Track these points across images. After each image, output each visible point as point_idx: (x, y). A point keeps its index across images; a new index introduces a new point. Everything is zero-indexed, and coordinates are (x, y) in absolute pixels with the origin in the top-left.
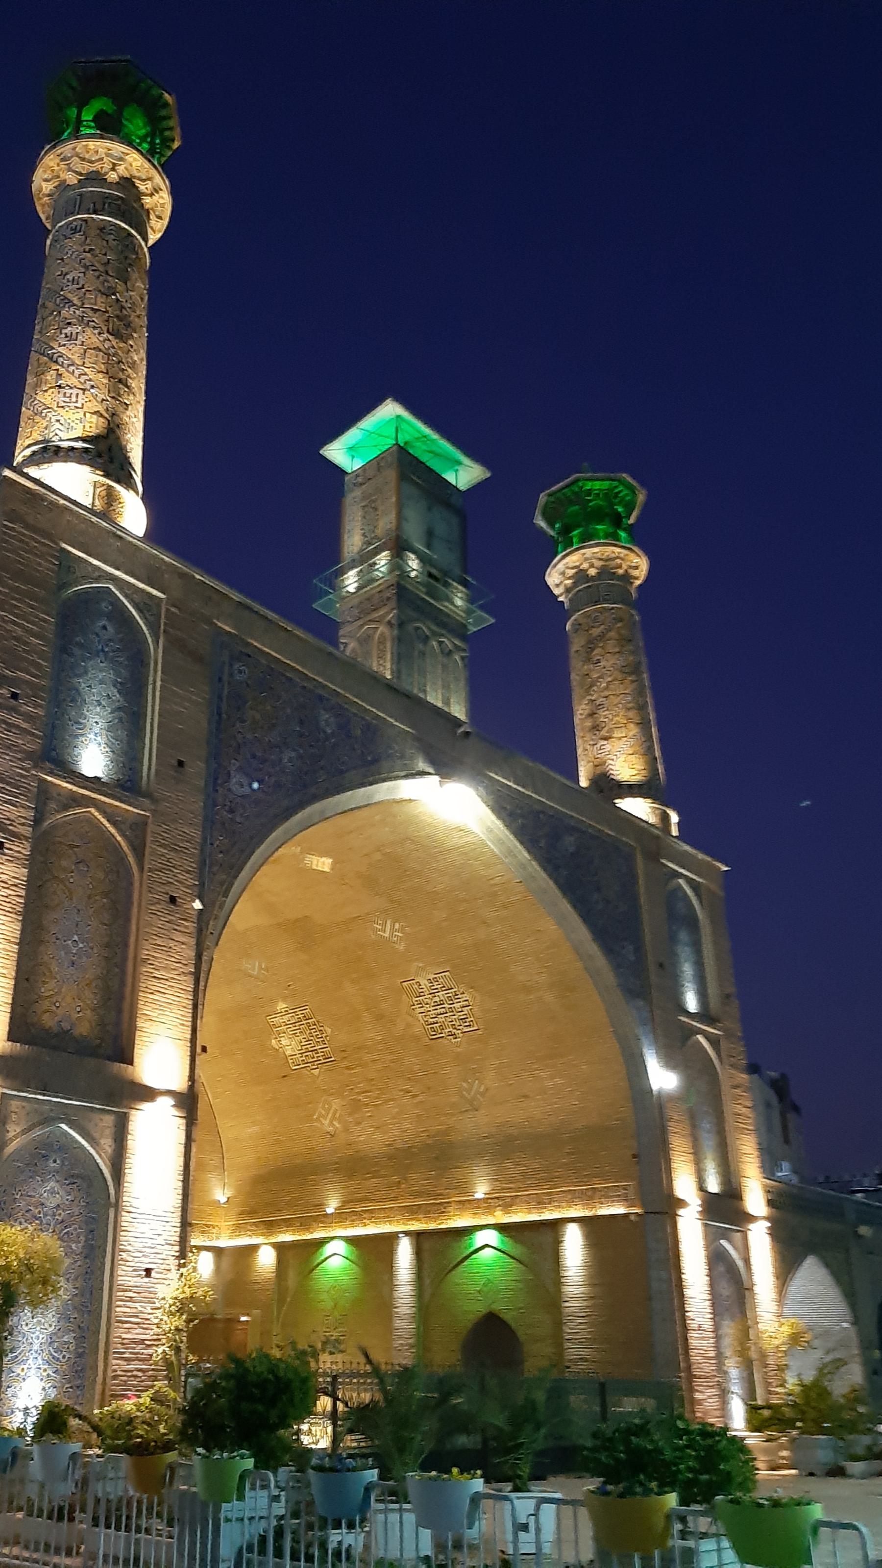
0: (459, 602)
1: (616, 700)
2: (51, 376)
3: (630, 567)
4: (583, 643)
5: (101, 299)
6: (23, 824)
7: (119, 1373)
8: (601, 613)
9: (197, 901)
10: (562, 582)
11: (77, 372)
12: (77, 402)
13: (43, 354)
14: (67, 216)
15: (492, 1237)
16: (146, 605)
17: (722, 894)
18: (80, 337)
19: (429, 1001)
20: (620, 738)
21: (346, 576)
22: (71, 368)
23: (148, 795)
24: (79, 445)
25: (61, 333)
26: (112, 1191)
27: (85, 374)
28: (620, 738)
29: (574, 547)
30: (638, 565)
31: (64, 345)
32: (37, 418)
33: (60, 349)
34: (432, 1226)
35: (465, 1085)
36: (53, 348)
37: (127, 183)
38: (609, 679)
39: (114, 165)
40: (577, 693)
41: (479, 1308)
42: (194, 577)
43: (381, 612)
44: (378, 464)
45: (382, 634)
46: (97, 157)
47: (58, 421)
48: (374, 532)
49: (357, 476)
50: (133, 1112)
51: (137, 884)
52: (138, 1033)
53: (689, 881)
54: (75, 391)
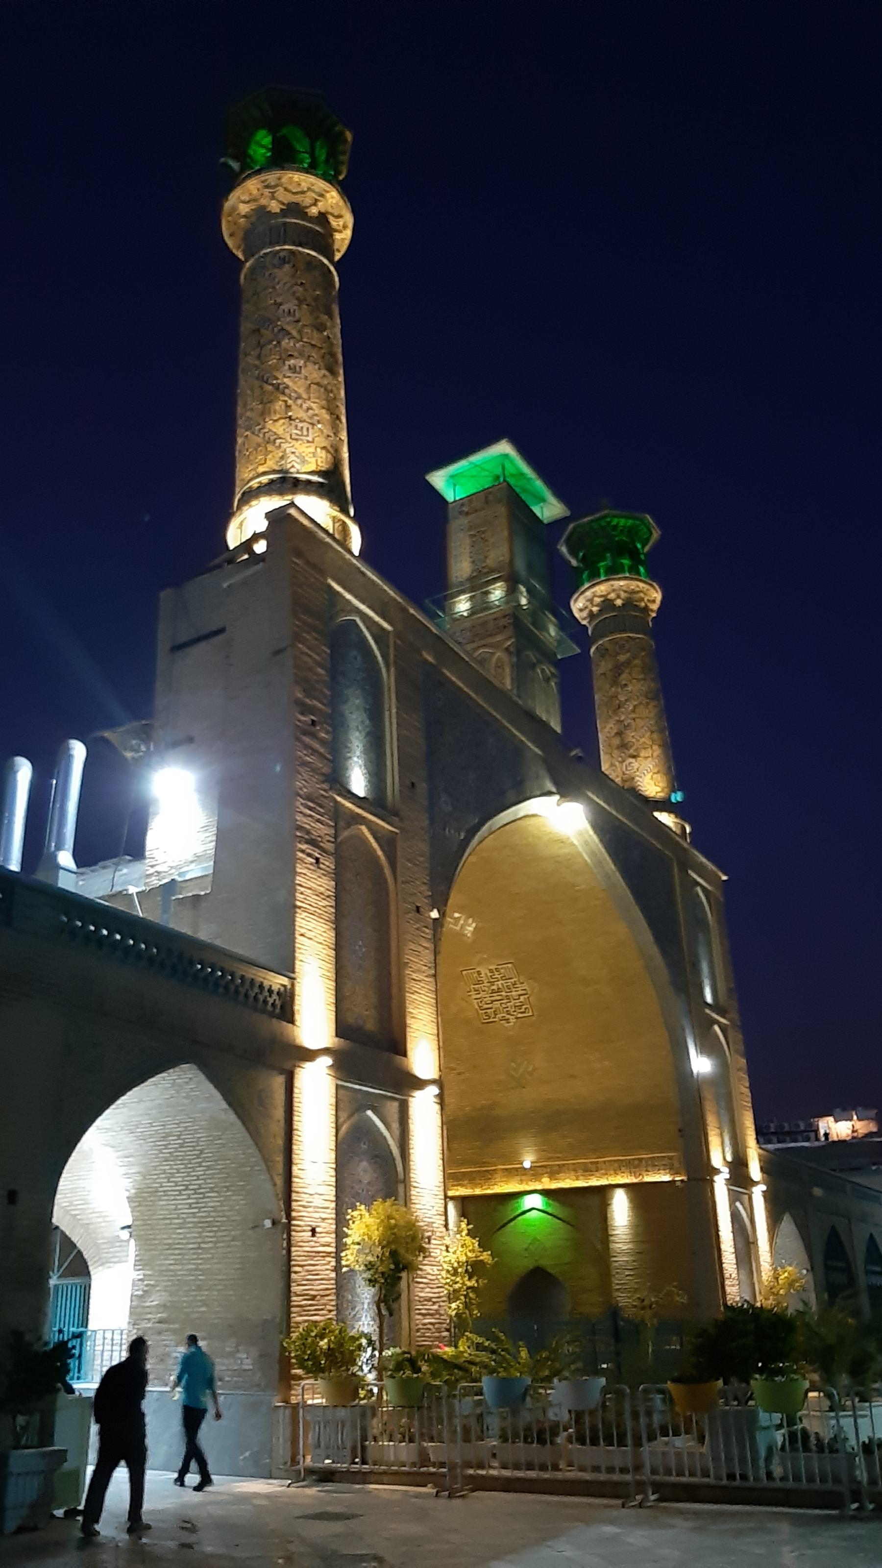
0: (553, 633)
1: (640, 722)
2: (279, 405)
3: (649, 601)
4: (610, 666)
5: (316, 334)
6: (328, 841)
7: (421, 1326)
8: (627, 641)
9: (435, 911)
10: (586, 608)
11: (305, 406)
12: (308, 436)
13: (267, 382)
14: (272, 244)
15: (535, 1201)
16: (380, 635)
17: (722, 900)
18: (303, 371)
19: (486, 989)
20: (646, 758)
21: (457, 599)
22: (299, 402)
23: (396, 814)
24: (315, 478)
25: (284, 364)
26: (400, 1168)
27: (312, 409)
28: (646, 758)
29: (603, 578)
30: (654, 596)
31: (289, 377)
32: (270, 447)
33: (286, 380)
34: (478, 1192)
35: (513, 1064)
36: (277, 379)
37: (323, 218)
38: (635, 703)
39: (316, 200)
40: (600, 712)
41: (527, 1264)
42: (408, 611)
43: (499, 638)
44: (486, 498)
45: (499, 659)
46: (300, 190)
47: (293, 453)
48: (484, 562)
49: (463, 505)
50: (411, 1099)
51: (392, 896)
52: (408, 1030)
53: (704, 889)
54: (305, 425)
